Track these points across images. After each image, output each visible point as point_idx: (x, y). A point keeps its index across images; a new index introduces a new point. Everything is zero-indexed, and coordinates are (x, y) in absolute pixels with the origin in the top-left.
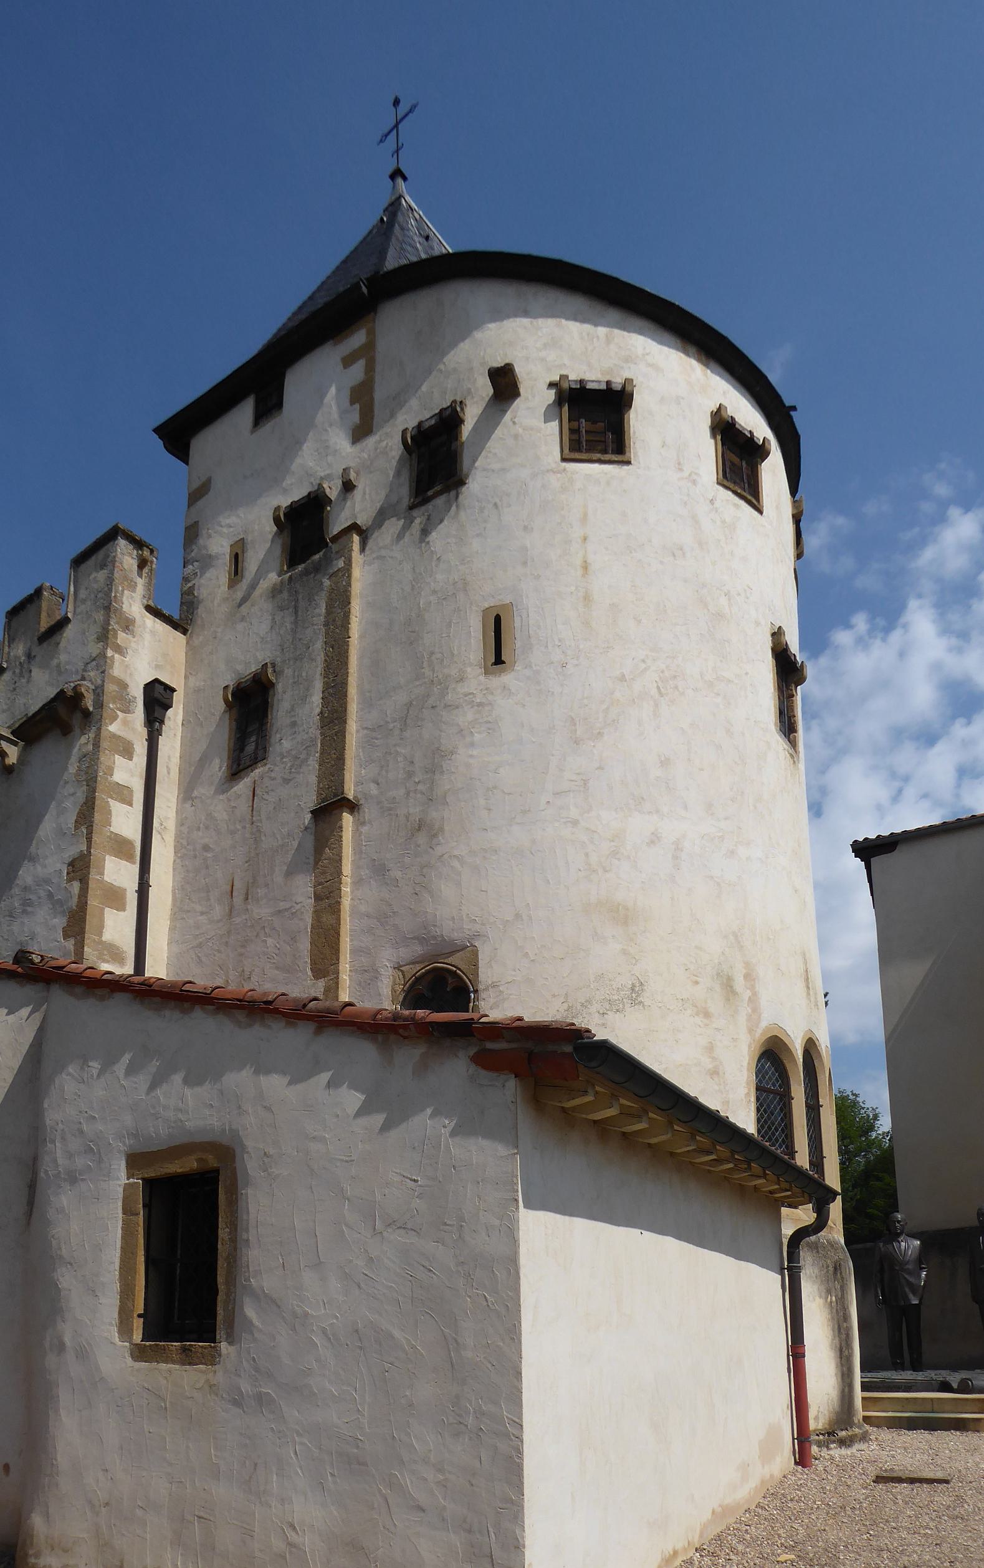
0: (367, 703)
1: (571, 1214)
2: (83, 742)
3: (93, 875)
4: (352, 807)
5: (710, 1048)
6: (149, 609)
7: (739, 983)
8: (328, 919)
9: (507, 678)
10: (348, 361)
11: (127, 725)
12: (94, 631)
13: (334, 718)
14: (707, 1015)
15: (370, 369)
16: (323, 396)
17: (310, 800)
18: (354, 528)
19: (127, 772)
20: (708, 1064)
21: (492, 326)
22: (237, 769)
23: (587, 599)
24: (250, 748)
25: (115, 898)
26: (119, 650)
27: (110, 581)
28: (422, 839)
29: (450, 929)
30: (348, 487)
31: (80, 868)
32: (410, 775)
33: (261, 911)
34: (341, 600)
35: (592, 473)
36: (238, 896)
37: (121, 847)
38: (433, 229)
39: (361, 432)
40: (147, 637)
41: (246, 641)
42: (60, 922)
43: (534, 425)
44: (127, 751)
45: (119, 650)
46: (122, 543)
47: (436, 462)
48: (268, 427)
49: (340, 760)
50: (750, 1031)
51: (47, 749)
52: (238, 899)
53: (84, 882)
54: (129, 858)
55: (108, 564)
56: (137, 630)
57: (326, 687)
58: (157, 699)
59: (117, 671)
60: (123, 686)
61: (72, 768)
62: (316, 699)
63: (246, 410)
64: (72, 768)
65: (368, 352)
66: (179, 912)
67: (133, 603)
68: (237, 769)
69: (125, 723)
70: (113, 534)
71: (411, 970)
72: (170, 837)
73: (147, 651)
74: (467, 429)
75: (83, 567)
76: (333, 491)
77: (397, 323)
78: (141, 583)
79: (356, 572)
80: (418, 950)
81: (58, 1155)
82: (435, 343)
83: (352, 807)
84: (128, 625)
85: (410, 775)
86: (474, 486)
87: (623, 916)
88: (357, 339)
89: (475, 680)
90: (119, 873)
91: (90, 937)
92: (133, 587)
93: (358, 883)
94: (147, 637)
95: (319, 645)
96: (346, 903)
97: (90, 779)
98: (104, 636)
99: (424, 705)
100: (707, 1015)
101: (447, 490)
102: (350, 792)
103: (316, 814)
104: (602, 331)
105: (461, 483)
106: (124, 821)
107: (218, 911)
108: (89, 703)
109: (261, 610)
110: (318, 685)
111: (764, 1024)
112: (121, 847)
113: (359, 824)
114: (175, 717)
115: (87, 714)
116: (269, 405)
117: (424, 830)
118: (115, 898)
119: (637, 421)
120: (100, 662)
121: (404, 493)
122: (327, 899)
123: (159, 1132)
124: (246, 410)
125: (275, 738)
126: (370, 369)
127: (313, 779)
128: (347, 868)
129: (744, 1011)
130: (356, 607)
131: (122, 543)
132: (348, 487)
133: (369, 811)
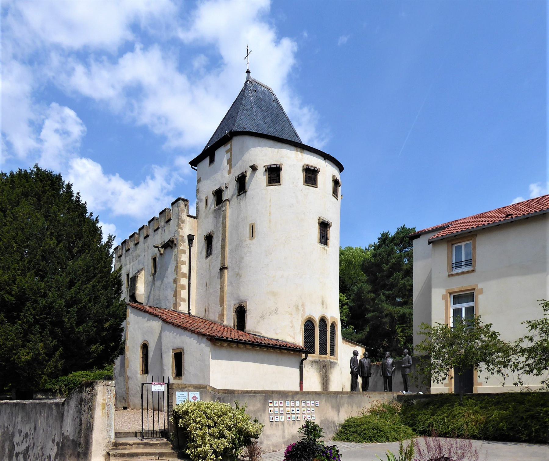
0: (230, 244)
1: (222, 360)
2: (175, 251)
3: (178, 283)
4: (227, 268)
5: (292, 322)
6: (188, 216)
7: (300, 307)
8: (222, 294)
9: (254, 241)
10: (227, 152)
11: (184, 246)
12: (176, 223)
13: (223, 247)
14: (291, 314)
15: (231, 153)
16: (223, 160)
17: (219, 266)
18: (226, 200)
19: (184, 257)
20: (291, 325)
21: (252, 149)
22: (207, 256)
23: (270, 221)
24: (209, 251)
25: (183, 287)
26: (181, 228)
27: (179, 212)
28: (238, 277)
29: (243, 298)
30: (227, 188)
31: (176, 281)
32: (236, 262)
33: (211, 290)
34: (224, 218)
35: (273, 188)
36: (208, 286)
37: (184, 275)
38: (236, 128)
39: (229, 172)
40: (188, 223)
41: (208, 225)
42: (173, 293)
43: (261, 177)
44: (184, 252)
45: (181, 228)
46: (181, 201)
47: (242, 184)
48: (212, 166)
49: (224, 257)
50: (302, 317)
51: (169, 250)
52: (208, 287)
53: (176, 284)
54: (186, 277)
55: (178, 207)
56: (185, 222)
57: (222, 239)
58: (191, 238)
59: (181, 234)
60: (183, 237)
61: (173, 257)
62: (220, 242)
63: (207, 160)
64: (173, 257)
65: (230, 151)
66: (197, 288)
67: (184, 216)
68: (207, 256)
69: (184, 246)
70: (178, 200)
71: (237, 306)
72: (195, 271)
73: (188, 227)
74: (247, 178)
75: (174, 206)
76: (224, 189)
77: (237, 141)
78: (185, 210)
79: (227, 211)
80: (238, 302)
81: (164, 349)
82: (242, 152)
83: (227, 268)
84: (183, 222)
85: (236, 262)
86: (248, 193)
87: (274, 294)
88: (228, 146)
89: (248, 241)
90: (184, 281)
91: (178, 297)
92: (184, 212)
93: (228, 286)
94: (188, 223)
95: (221, 228)
96: (226, 290)
97: (177, 260)
98: (178, 225)
99: (239, 246)
100: (291, 314)
101: (244, 193)
102: (227, 265)
103: (220, 269)
104: (276, 150)
105: (246, 192)
106: (184, 269)
107: (204, 289)
108: (175, 242)
109: (211, 216)
110: (221, 239)
111: (306, 315)
112: (184, 275)
113: (228, 272)
114: (195, 241)
115: (175, 245)
116: (212, 161)
117: (238, 275)
118: (183, 287)
119: (283, 175)
120: (177, 232)
121: (237, 191)
122: (222, 289)
123: (176, 346)
124: (207, 160)
125: (213, 249)
126: (231, 156)
127: (220, 261)
128: (226, 282)
129: (301, 312)
130: (228, 220)
131: (181, 201)
132: (227, 188)
133: (230, 269)
